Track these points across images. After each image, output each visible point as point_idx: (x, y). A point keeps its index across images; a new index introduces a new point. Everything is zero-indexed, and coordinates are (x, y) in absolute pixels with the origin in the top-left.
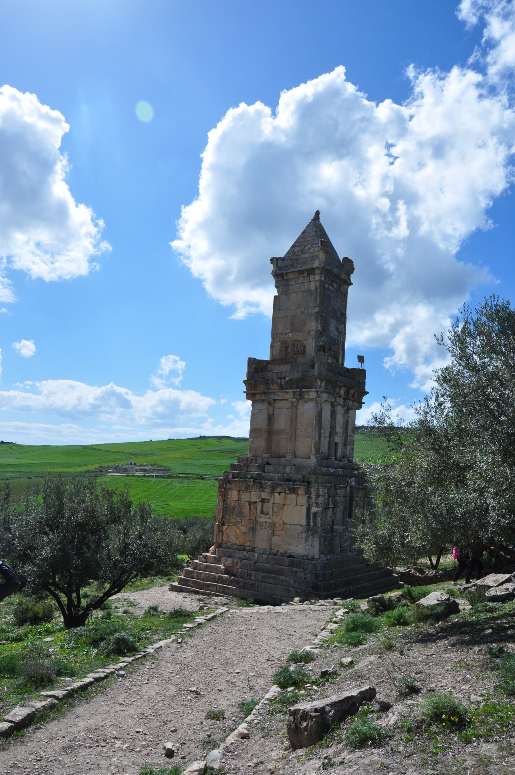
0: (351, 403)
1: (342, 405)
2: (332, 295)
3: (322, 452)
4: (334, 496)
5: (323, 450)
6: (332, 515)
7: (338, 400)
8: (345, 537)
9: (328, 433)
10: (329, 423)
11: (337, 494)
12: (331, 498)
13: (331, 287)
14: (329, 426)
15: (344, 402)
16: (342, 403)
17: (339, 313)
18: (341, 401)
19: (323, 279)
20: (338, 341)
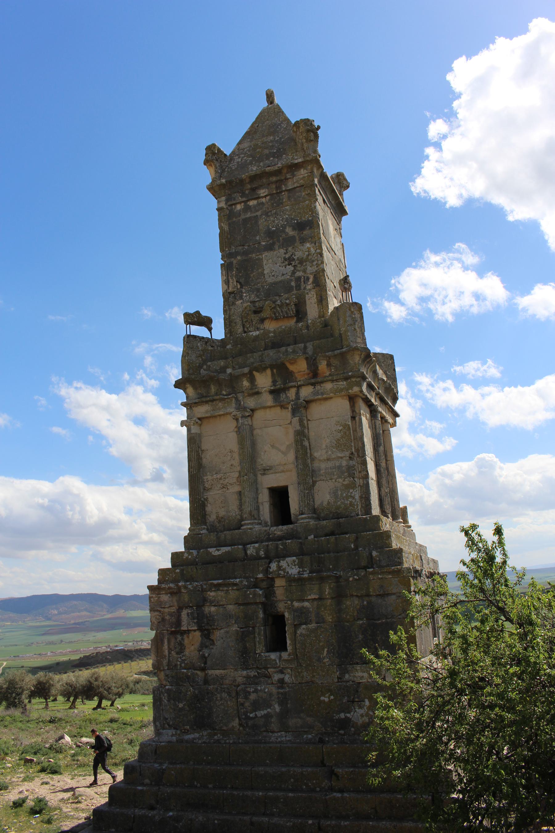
0: (306, 392)
1: (283, 407)
2: (259, 213)
3: (220, 520)
4: (199, 607)
5: (222, 513)
6: (203, 646)
7: (251, 403)
8: (253, 697)
9: (237, 475)
10: (236, 456)
11: (205, 600)
12: (184, 613)
13: (252, 203)
14: (236, 462)
15: (276, 399)
16: (270, 403)
19: (223, 205)
20: (298, 279)
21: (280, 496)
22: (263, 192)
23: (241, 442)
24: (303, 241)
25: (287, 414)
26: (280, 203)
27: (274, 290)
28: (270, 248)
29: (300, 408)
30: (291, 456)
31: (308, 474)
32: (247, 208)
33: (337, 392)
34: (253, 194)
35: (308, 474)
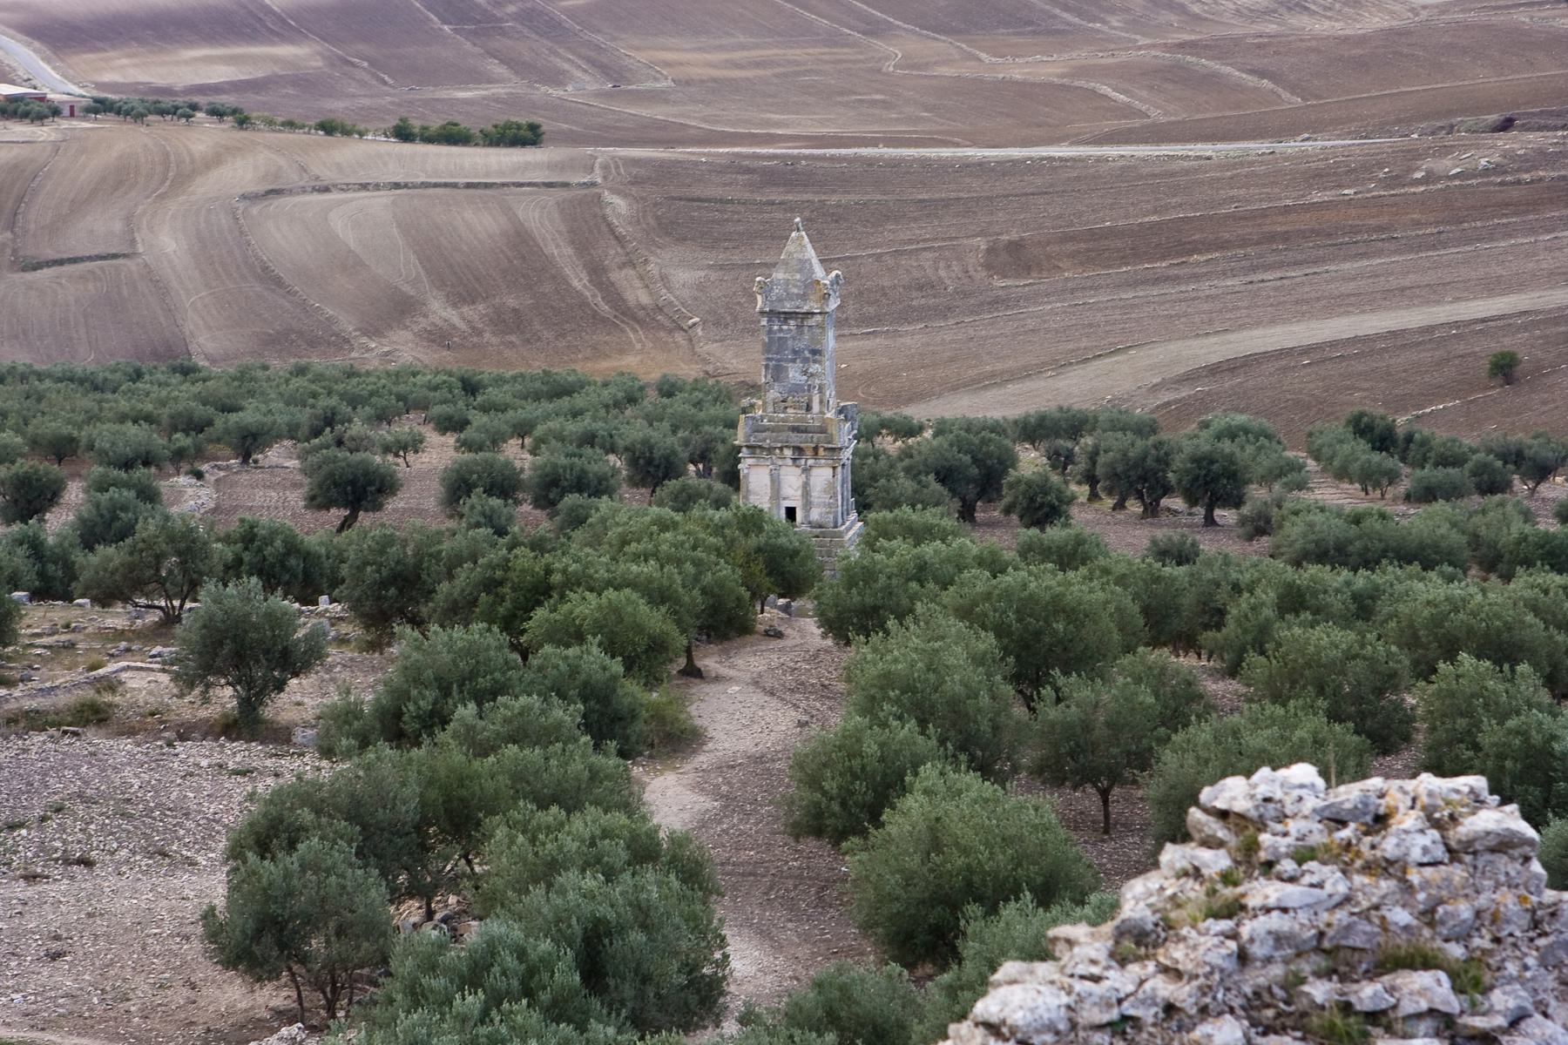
0: (810, 462)
17: (807, 354)
18: (790, 462)
21: (791, 513)
22: (792, 322)
23: (772, 481)
24: (815, 362)
25: (799, 471)
26: (802, 333)
27: (796, 389)
28: (794, 361)
29: (807, 471)
30: (800, 492)
31: (808, 505)
32: (781, 330)
33: (827, 465)
34: (785, 322)
35: (808, 505)
